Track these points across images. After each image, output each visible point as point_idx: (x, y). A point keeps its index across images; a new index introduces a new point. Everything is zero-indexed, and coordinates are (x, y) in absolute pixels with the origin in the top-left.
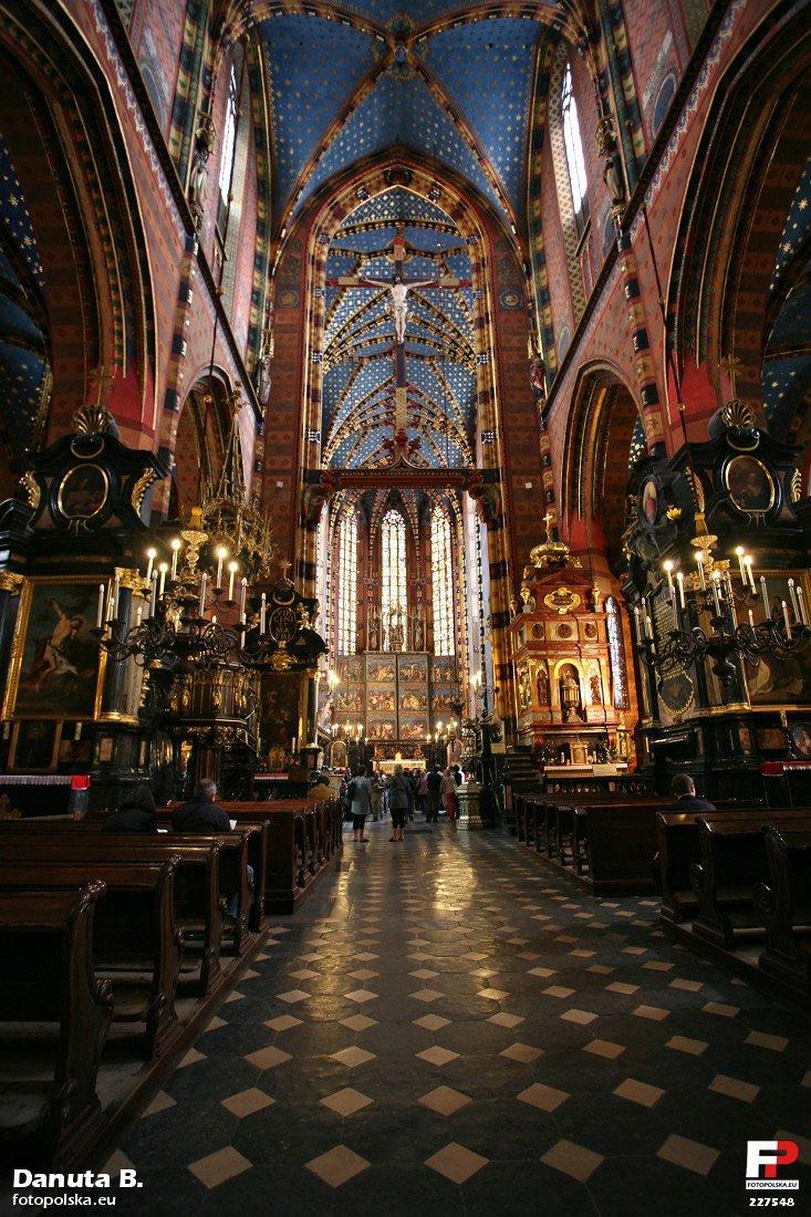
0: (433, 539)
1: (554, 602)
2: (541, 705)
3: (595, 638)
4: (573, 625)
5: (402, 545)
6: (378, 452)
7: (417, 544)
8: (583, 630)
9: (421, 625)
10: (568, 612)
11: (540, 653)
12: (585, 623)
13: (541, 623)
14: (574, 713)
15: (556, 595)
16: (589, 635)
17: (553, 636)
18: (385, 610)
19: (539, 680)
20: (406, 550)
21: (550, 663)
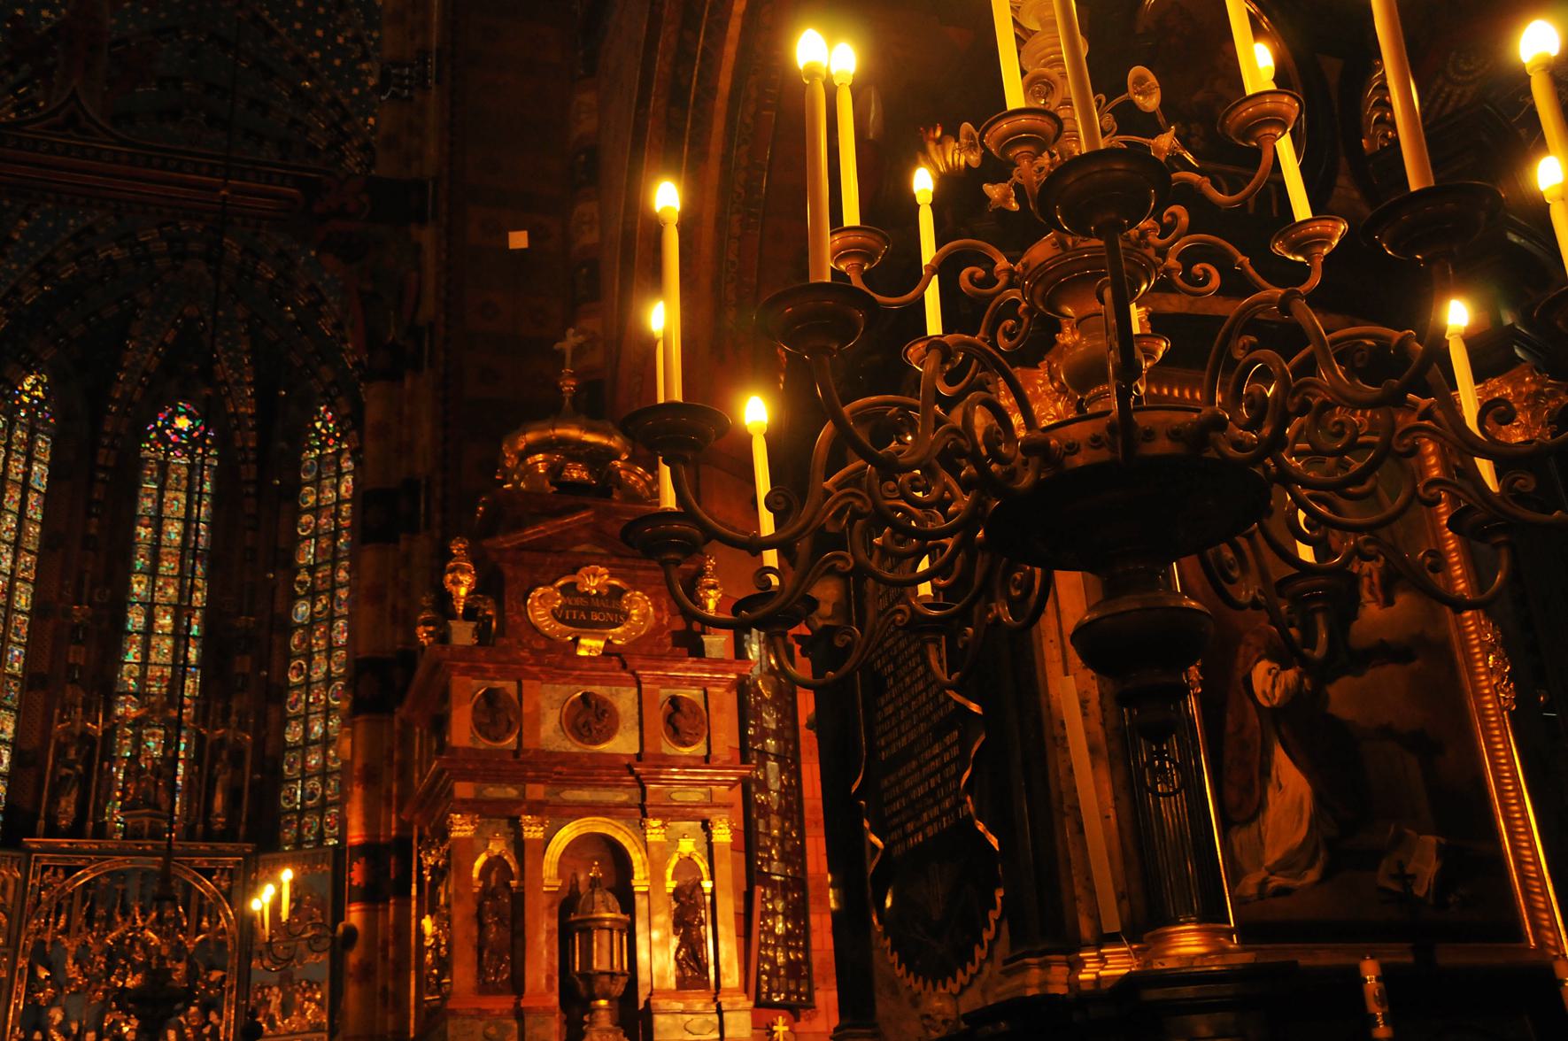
1: (556, 615)
2: (484, 988)
3: (699, 749)
4: (624, 700)
8: (656, 719)
9: (237, 758)
10: (609, 652)
11: (493, 792)
12: (665, 693)
13: (510, 687)
14: (604, 1020)
15: (569, 590)
16: (678, 737)
17: (550, 732)
18: (127, 709)
19: (486, 893)
21: (532, 832)
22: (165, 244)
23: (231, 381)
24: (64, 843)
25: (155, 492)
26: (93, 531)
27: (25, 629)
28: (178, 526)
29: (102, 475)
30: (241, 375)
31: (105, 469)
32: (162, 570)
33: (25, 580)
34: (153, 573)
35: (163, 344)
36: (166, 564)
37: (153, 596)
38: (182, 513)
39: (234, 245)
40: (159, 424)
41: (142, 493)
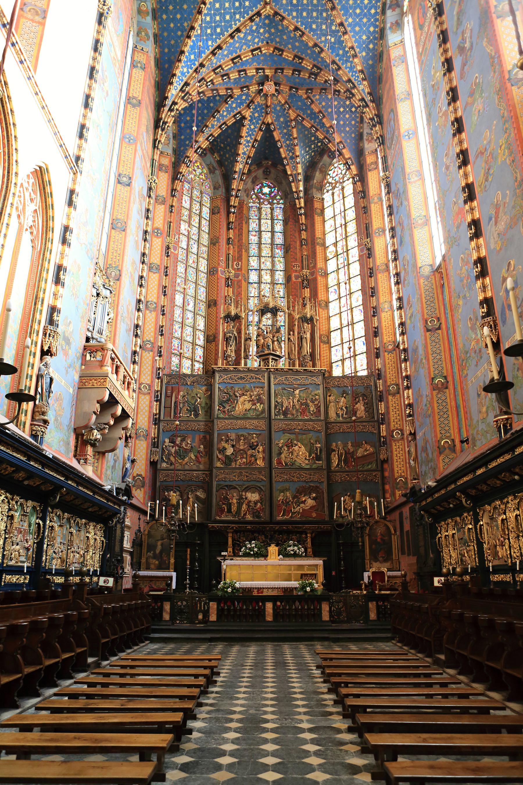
0: (328, 213)
5: (279, 227)
6: (238, 30)
7: (303, 219)
20: (285, 233)
22: (254, 71)
23: (288, 157)
24: (231, 368)
25: (257, 221)
26: (231, 236)
27: (205, 280)
28: (269, 234)
29: (233, 210)
30: (293, 153)
31: (235, 207)
32: (263, 254)
33: (204, 258)
34: (260, 256)
35: (256, 140)
36: (265, 252)
37: (260, 266)
38: (270, 230)
39: (289, 55)
40: (256, 191)
41: (251, 221)
